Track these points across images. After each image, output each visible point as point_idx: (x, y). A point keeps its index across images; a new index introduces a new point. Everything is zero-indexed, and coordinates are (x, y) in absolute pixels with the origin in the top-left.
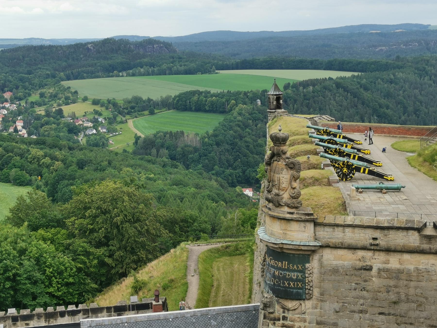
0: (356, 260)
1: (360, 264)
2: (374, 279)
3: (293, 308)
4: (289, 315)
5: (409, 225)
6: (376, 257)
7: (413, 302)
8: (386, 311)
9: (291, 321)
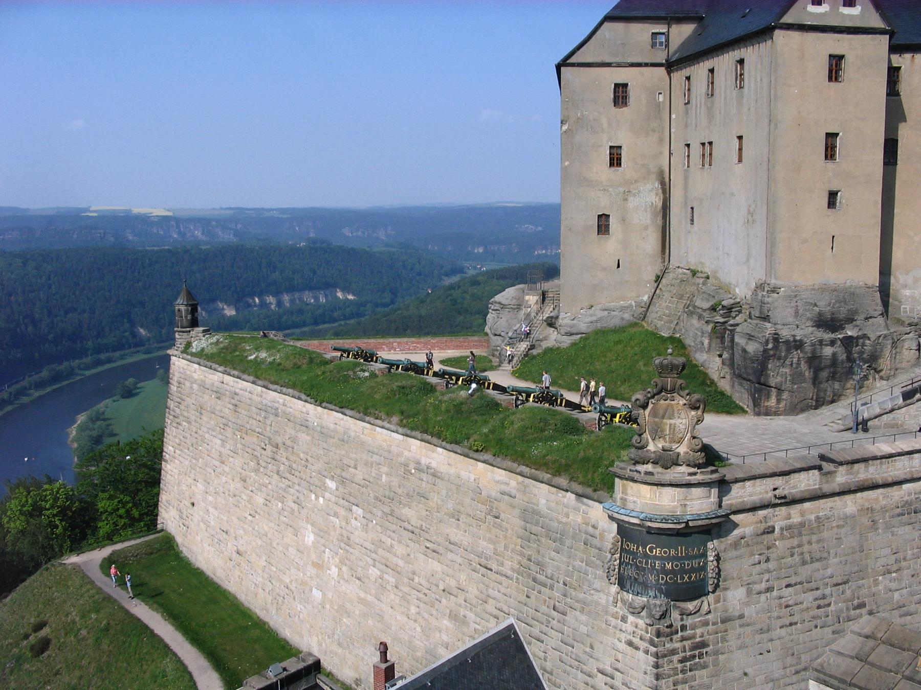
0: (756, 523)
1: (762, 526)
2: (777, 543)
3: (695, 611)
4: (689, 621)
6: (777, 513)
7: (820, 560)
8: (793, 580)
9: (692, 630)
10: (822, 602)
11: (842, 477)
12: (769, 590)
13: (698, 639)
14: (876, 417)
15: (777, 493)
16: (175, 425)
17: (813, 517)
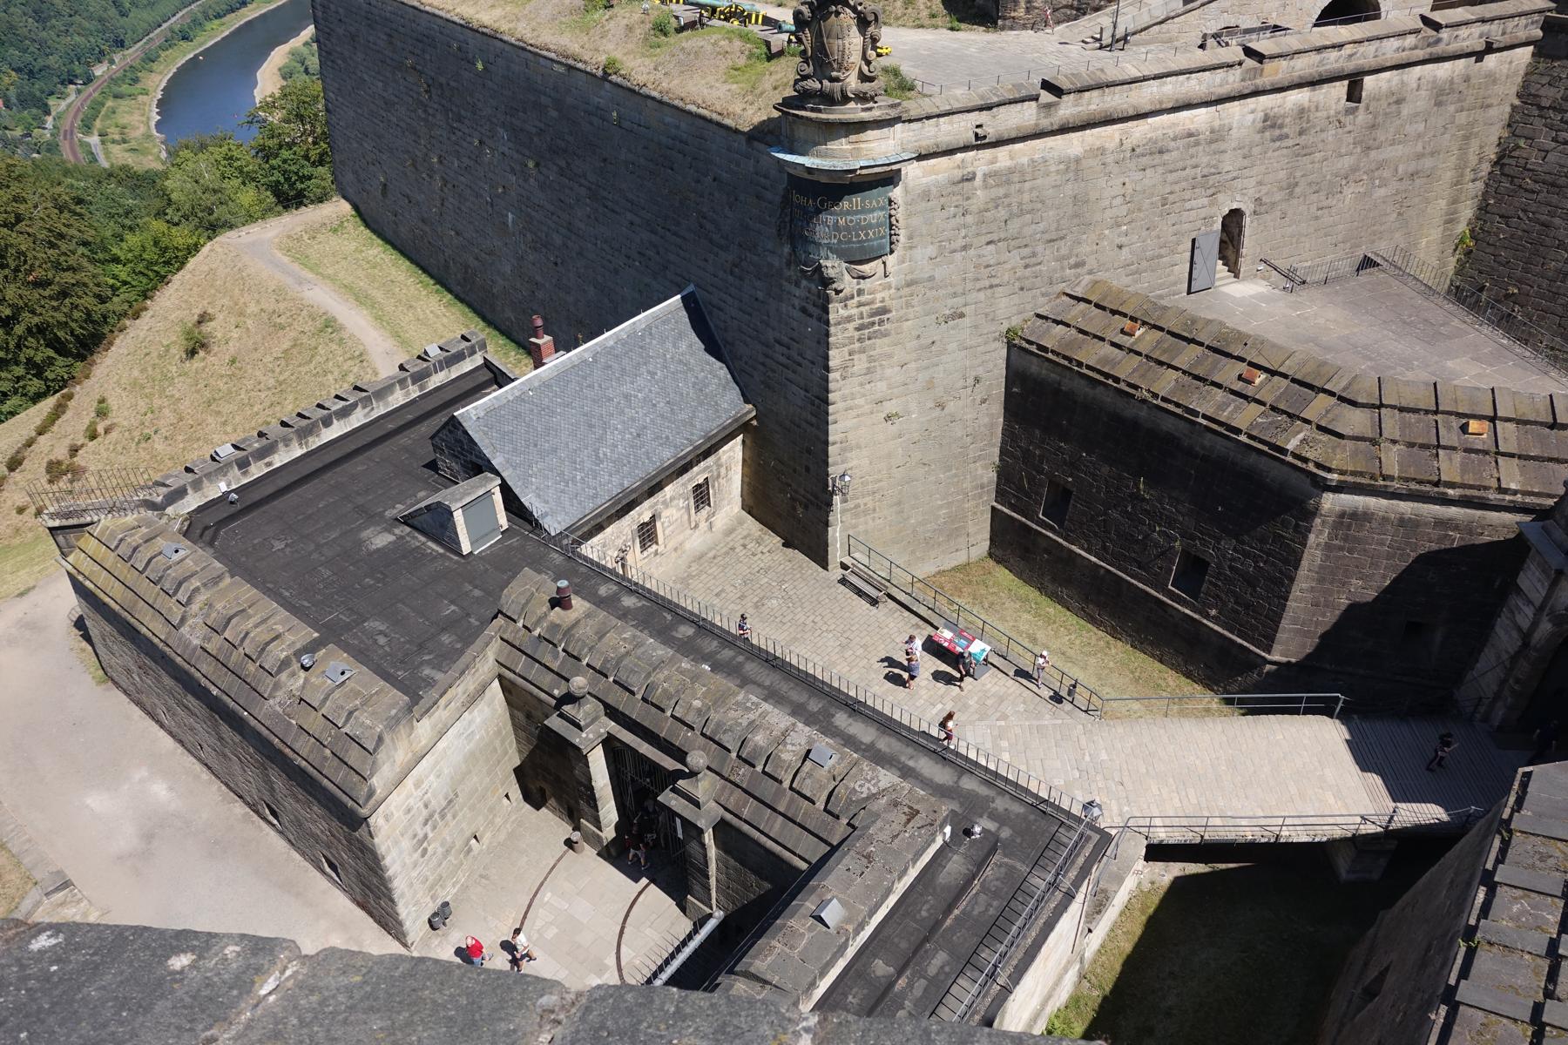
1: (958, 174)
2: (979, 192)
4: (864, 284)
5: (1024, 93)
7: (1029, 212)
8: (995, 237)
10: (1033, 260)
11: (1068, 109)
12: (965, 248)
13: (878, 305)
14: (1142, 31)
15: (979, 131)
16: (329, 63)
17: (1025, 160)
